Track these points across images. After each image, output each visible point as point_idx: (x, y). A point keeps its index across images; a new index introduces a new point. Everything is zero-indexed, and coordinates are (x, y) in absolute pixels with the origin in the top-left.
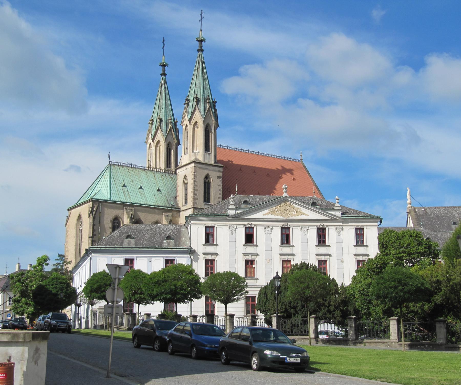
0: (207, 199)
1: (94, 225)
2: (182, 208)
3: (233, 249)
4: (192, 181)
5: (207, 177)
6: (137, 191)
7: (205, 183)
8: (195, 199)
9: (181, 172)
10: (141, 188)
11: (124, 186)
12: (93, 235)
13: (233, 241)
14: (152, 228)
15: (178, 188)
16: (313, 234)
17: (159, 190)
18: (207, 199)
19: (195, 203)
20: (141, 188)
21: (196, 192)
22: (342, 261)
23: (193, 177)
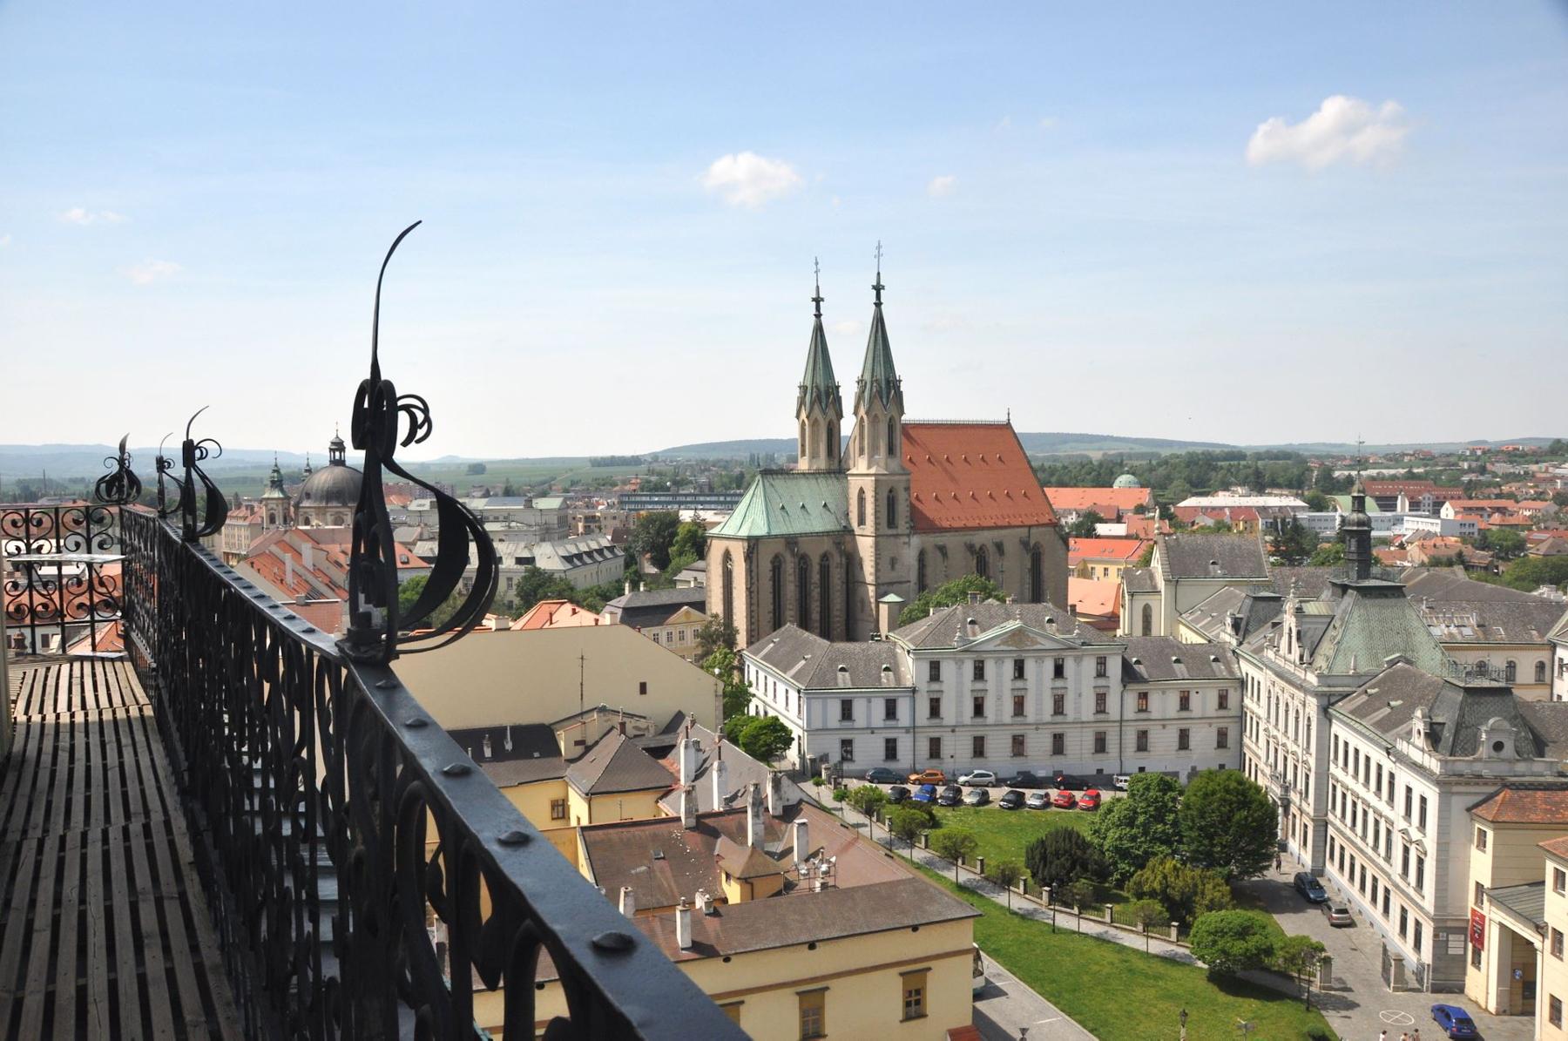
0: (891, 523)
1: (751, 571)
2: (857, 531)
3: (960, 683)
4: (873, 500)
5: (891, 491)
6: (799, 511)
7: (888, 497)
8: (877, 524)
9: (854, 484)
10: (803, 507)
11: (783, 508)
12: (752, 584)
13: (960, 675)
14: (863, 650)
15: (851, 501)
16: (1049, 667)
17: (825, 505)
18: (891, 523)
19: (876, 529)
20: (803, 507)
21: (878, 515)
22: (1080, 695)
23: (873, 494)
